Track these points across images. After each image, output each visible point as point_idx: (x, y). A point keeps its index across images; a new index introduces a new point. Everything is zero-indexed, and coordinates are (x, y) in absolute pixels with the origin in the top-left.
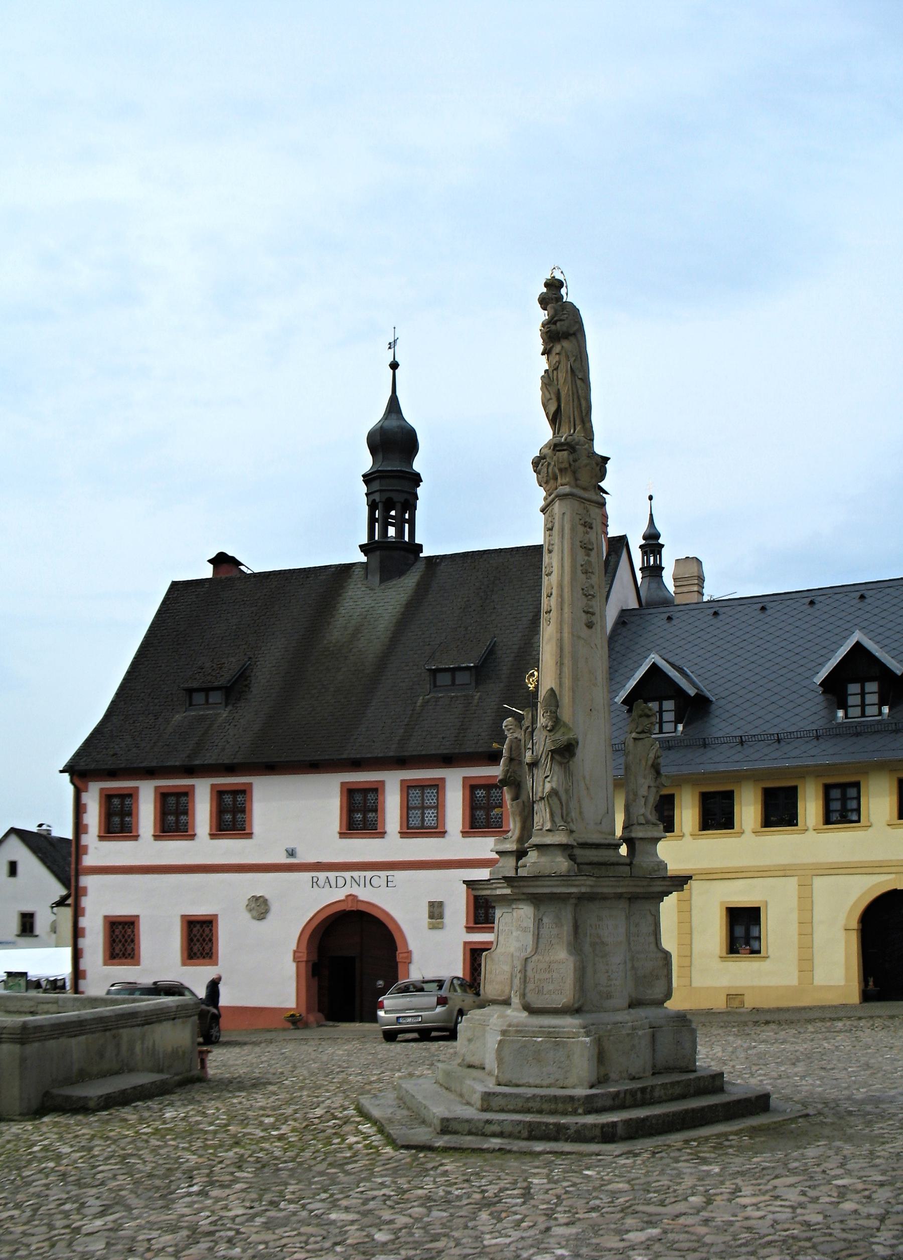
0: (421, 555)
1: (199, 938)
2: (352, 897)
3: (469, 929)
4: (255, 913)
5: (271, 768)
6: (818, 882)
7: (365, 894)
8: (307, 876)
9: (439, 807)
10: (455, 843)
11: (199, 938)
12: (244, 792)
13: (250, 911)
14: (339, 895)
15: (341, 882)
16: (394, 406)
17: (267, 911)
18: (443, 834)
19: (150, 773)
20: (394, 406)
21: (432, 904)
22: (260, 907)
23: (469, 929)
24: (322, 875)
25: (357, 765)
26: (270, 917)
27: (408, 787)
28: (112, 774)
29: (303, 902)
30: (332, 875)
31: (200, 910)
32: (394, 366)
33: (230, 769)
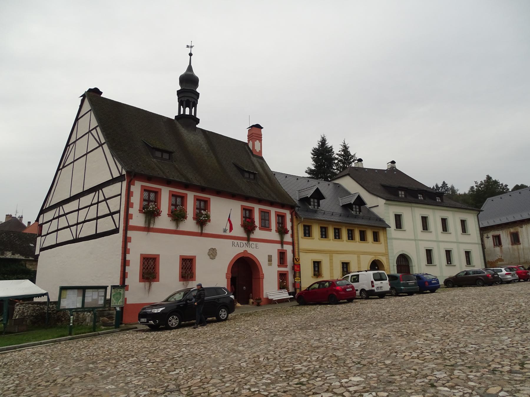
0: (197, 126)
1: (187, 267)
2: (245, 251)
3: (279, 266)
4: (211, 256)
5: (219, 193)
6: (361, 256)
7: (250, 251)
8: (230, 241)
9: (269, 220)
10: (273, 235)
11: (187, 267)
12: (206, 202)
13: (209, 255)
14: (241, 250)
15: (242, 246)
16: (190, 68)
17: (216, 255)
18: (270, 230)
19: (168, 183)
20: (190, 68)
21: (269, 256)
22: (213, 253)
23: (279, 266)
24: (236, 241)
25: (247, 199)
26: (216, 257)
27: (261, 211)
28: (149, 179)
29: (229, 251)
30: (239, 242)
31: (188, 253)
32: (191, 55)
33: (203, 190)
